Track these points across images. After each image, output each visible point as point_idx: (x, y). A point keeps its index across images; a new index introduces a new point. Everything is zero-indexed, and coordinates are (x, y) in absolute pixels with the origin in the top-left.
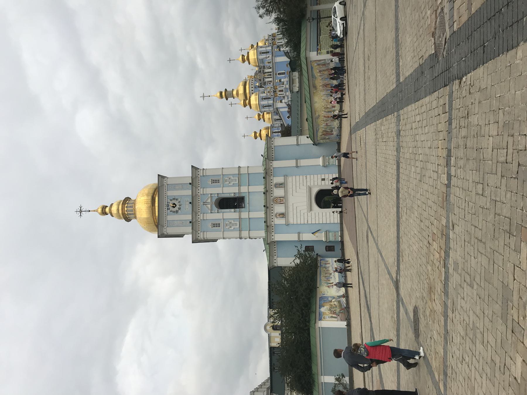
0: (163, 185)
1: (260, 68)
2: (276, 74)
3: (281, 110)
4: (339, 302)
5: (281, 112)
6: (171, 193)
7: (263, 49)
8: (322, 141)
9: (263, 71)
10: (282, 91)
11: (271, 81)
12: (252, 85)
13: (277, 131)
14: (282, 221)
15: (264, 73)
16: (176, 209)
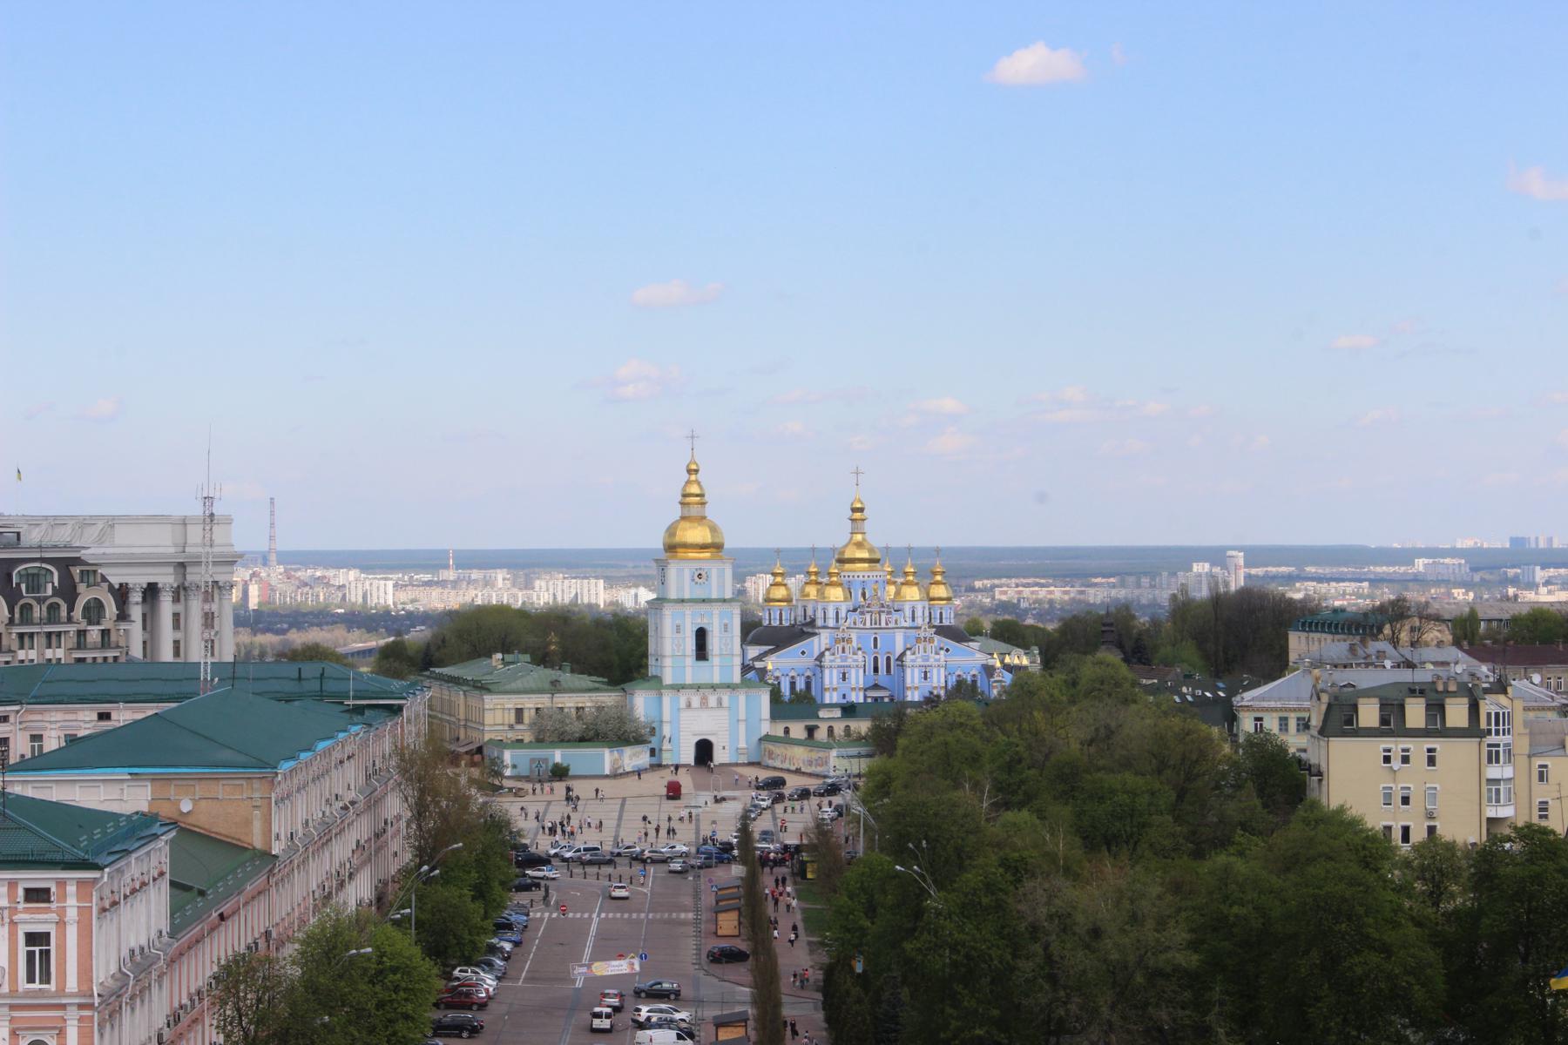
0: (724, 563)
1: (888, 606)
2: (876, 633)
3: (816, 639)
4: (619, 768)
5: (813, 641)
6: (714, 574)
7: (919, 613)
8: (763, 746)
9: (883, 612)
10: (843, 651)
11: (865, 624)
12: (869, 577)
13: (784, 618)
14: (683, 704)
15: (879, 613)
16: (697, 579)
